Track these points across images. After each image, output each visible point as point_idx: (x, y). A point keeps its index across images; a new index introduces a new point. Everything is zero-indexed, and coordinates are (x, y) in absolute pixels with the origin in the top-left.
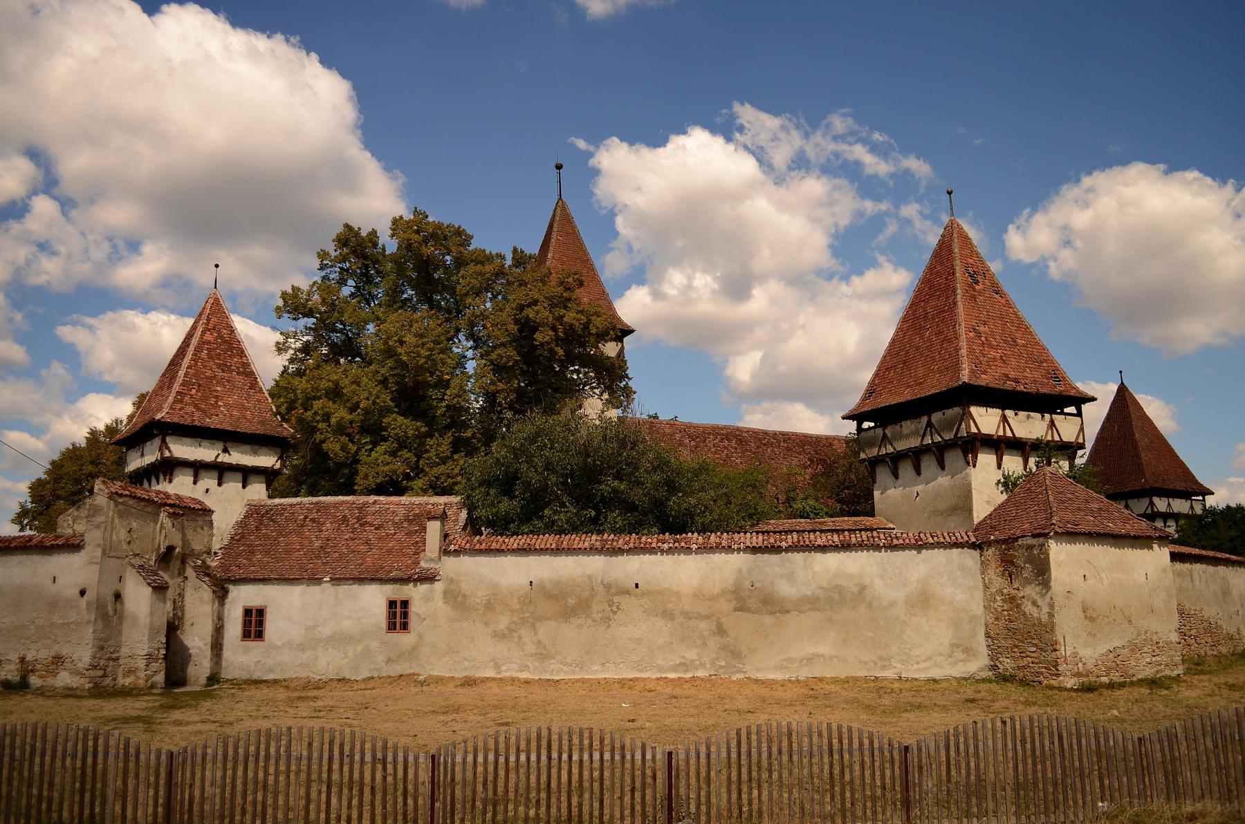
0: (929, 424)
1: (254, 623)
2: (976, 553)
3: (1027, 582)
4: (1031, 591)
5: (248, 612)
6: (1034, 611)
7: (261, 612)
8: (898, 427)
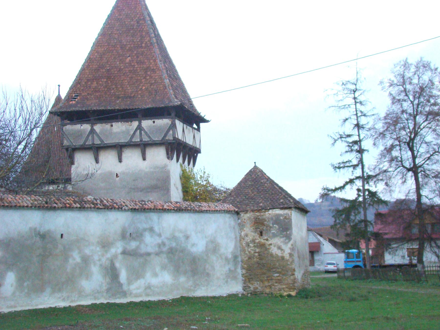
0: (139, 127)
2: (235, 216)
3: (274, 236)
4: (278, 241)
6: (279, 253)
8: (107, 126)
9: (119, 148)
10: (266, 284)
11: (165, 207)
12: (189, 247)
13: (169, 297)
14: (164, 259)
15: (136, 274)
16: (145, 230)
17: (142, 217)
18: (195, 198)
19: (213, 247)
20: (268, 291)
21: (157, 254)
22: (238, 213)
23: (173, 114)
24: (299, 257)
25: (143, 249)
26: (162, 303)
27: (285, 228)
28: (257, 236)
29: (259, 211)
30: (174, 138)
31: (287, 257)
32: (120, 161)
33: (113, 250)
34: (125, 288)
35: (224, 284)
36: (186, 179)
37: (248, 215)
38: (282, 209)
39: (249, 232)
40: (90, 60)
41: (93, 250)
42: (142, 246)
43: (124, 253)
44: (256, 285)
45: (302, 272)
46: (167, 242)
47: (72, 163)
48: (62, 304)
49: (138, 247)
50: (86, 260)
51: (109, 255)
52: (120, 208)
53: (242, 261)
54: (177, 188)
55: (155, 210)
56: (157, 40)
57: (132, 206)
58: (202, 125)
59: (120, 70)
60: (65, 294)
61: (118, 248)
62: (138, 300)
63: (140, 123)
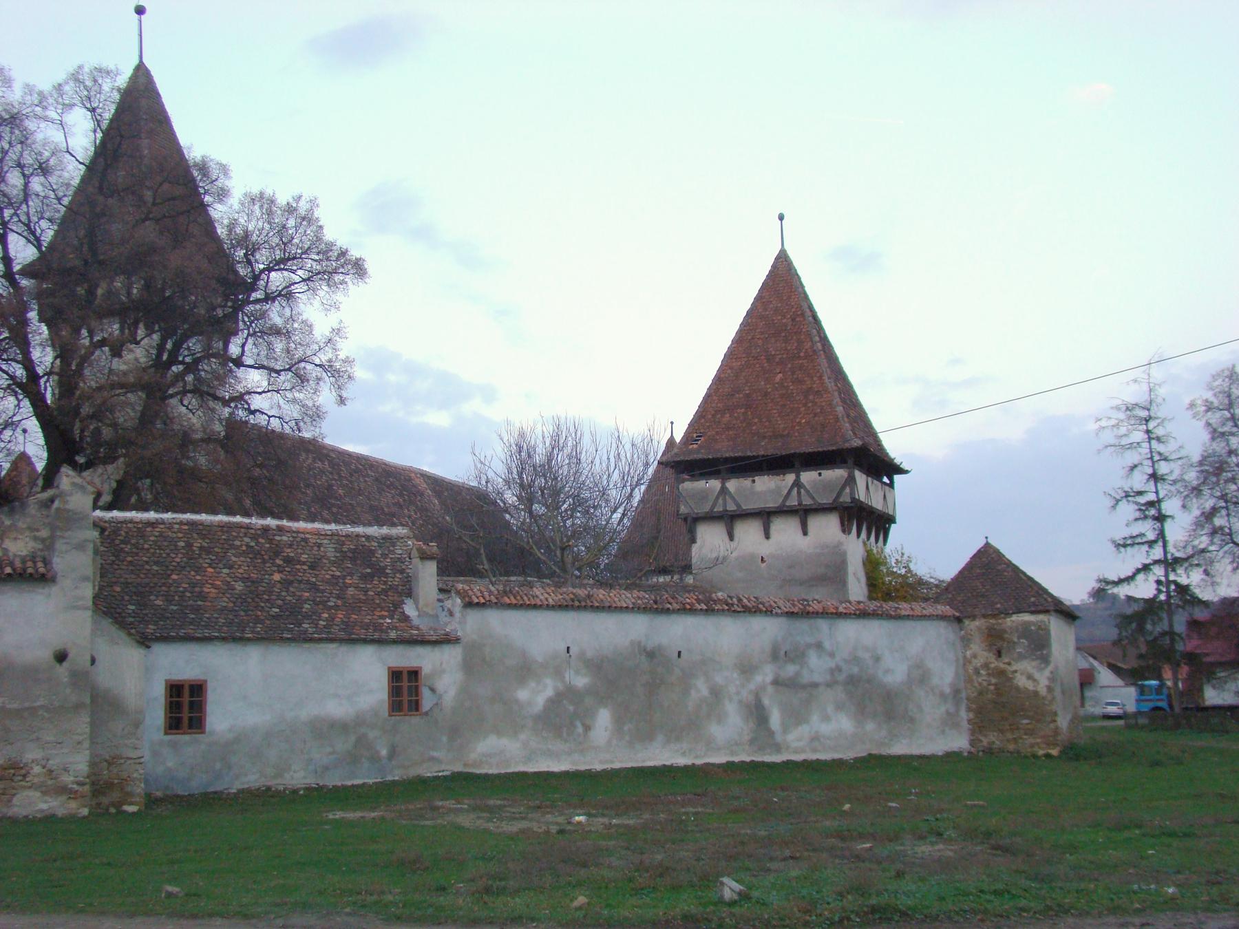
0: (797, 484)
1: (186, 705)
2: (956, 625)
3: (1021, 657)
4: (1027, 666)
5: (175, 689)
6: (1030, 685)
7: (198, 689)
8: (746, 482)
9: (766, 516)
10: (1009, 736)
11: (841, 609)
12: (880, 674)
13: (848, 755)
14: (839, 693)
15: (796, 717)
16: (809, 646)
17: (803, 625)
18: (887, 596)
19: (920, 676)
20: (1011, 747)
21: (829, 685)
22: (959, 620)
23: (850, 462)
24: (1063, 692)
25: (806, 678)
26: (839, 763)
27: (1039, 645)
28: (991, 657)
29: (994, 616)
30: (854, 500)
31: (1043, 691)
32: (767, 536)
33: (759, 679)
34: (779, 738)
35: (937, 734)
36: (873, 565)
37: (977, 623)
38: (1033, 613)
39: (980, 652)
40: (719, 380)
41: (728, 678)
42: (805, 672)
43: (776, 682)
44: (992, 738)
45: (1069, 717)
46: (844, 667)
47: (693, 540)
48: (682, 761)
49: (798, 674)
50: (717, 693)
51: (752, 686)
52: (769, 612)
53: (968, 699)
54: (858, 579)
55: (824, 614)
56: (823, 345)
57: (787, 607)
58: (896, 477)
59: (766, 394)
60: (685, 746)
61: (766, 675)
62: (798, 757)
63: (798, 476)
